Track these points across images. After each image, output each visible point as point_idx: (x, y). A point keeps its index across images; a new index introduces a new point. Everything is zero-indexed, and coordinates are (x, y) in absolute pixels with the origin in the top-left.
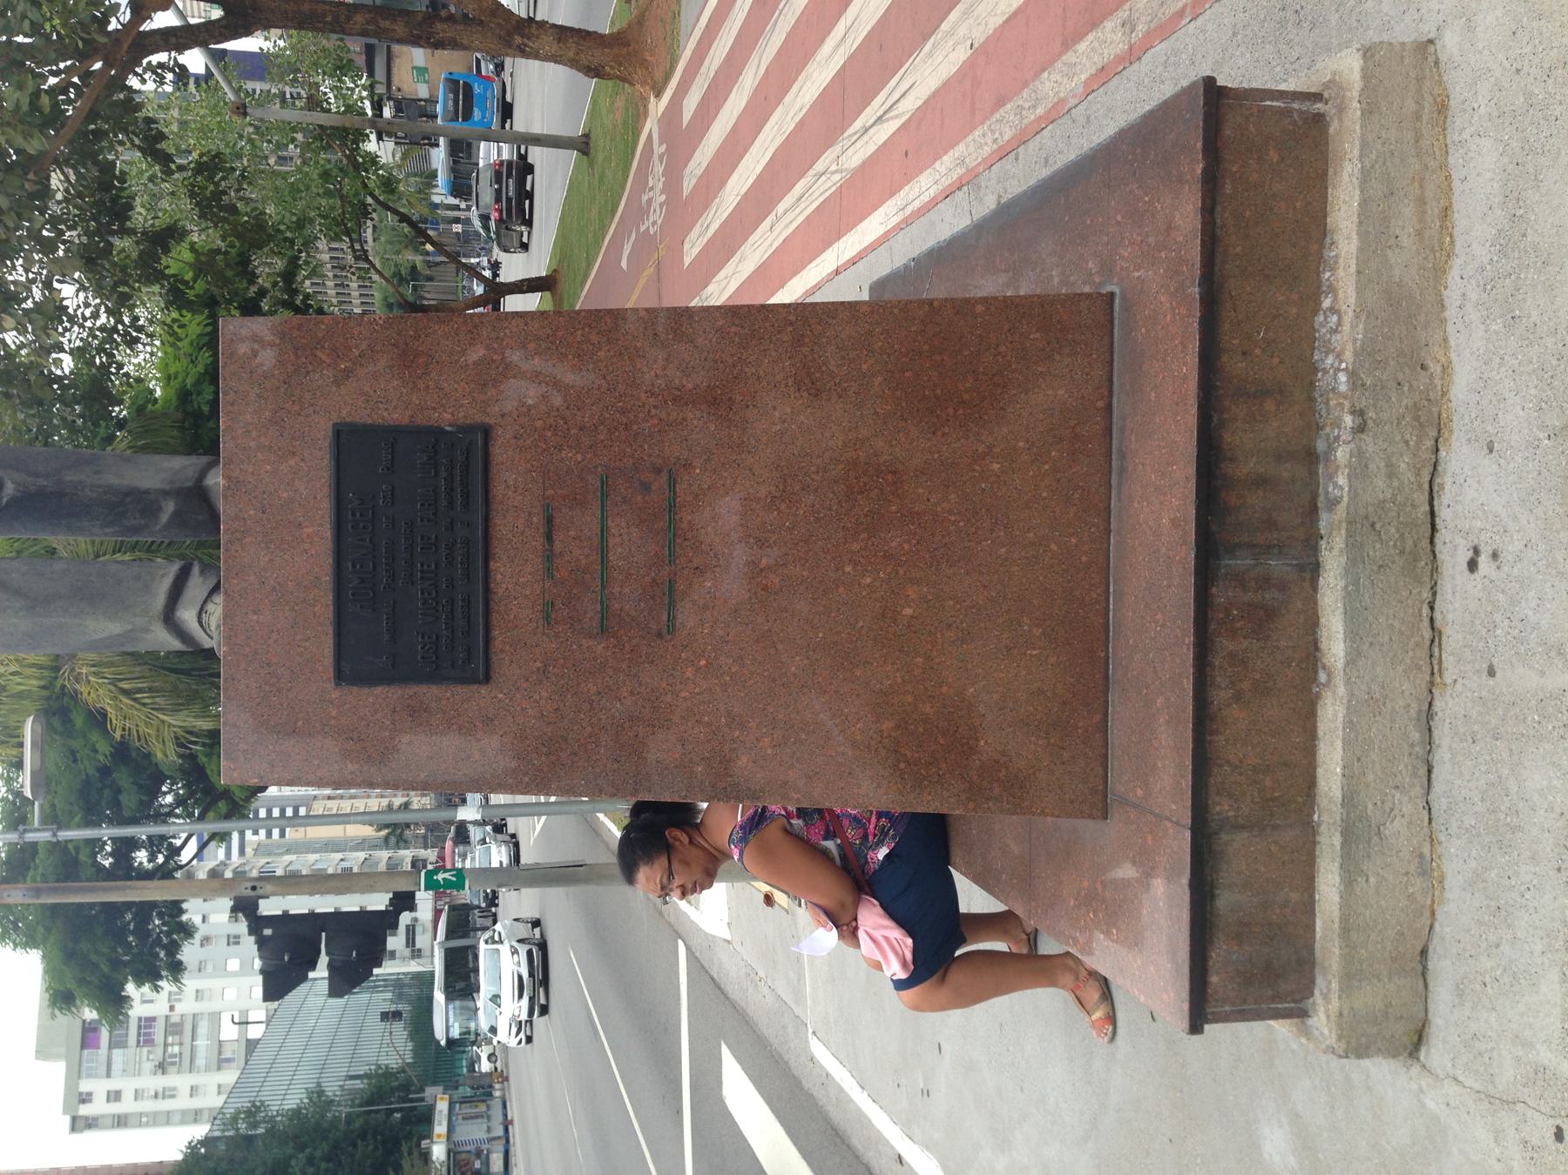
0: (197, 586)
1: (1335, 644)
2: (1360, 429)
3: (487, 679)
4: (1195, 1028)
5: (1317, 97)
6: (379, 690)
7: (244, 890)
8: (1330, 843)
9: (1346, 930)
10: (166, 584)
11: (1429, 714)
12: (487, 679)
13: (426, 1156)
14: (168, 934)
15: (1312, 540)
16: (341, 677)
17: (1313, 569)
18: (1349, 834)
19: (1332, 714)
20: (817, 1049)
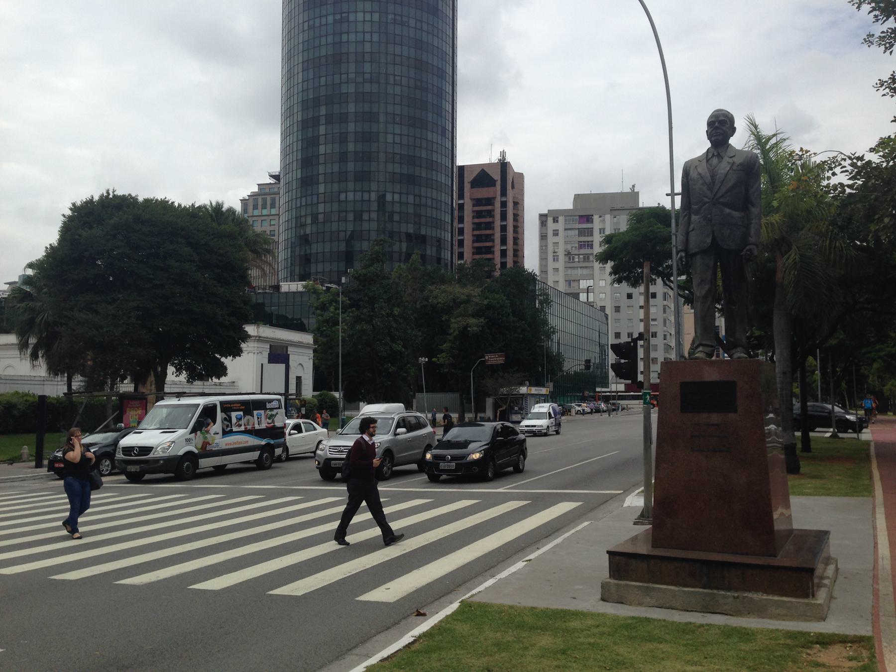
0: (708, 350)
1: (686, 589)
2: (734, 597)
4: (608, 552)
5: (813, 596)
7: (646, 336)
8: (646, 585)
9: (627, 585)
10: (709, 343)
11: (672, 609)
14: (634, 276)
15: (711, 588)
17: (704, 588)
18: (647, 587)
19: (673, 588)
20: (586, 524)
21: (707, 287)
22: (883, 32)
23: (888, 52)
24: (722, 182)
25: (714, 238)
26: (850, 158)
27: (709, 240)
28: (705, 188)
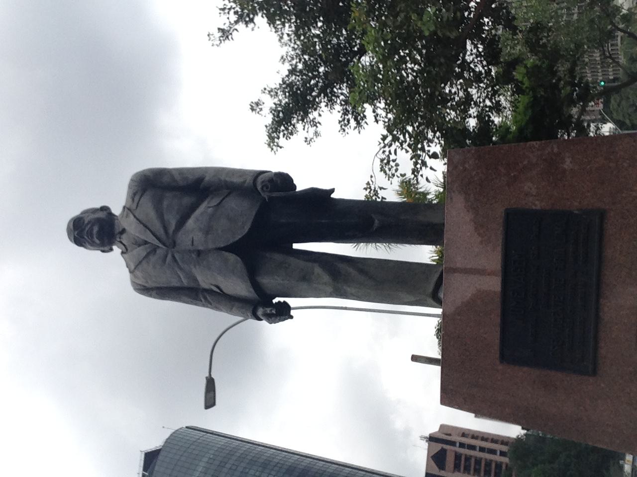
3: (594, 373)
6: (525, 369)
12: (594, 373)
13: (621, 468)
16: (503, 358)
21: (318, 270)
22: (304, 129)
23: (318, 125)
24: (146, 226)
25: (229, 249)
26: (384, 147)
27: (232, 257)
28: (153, 259)
